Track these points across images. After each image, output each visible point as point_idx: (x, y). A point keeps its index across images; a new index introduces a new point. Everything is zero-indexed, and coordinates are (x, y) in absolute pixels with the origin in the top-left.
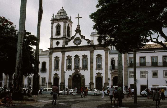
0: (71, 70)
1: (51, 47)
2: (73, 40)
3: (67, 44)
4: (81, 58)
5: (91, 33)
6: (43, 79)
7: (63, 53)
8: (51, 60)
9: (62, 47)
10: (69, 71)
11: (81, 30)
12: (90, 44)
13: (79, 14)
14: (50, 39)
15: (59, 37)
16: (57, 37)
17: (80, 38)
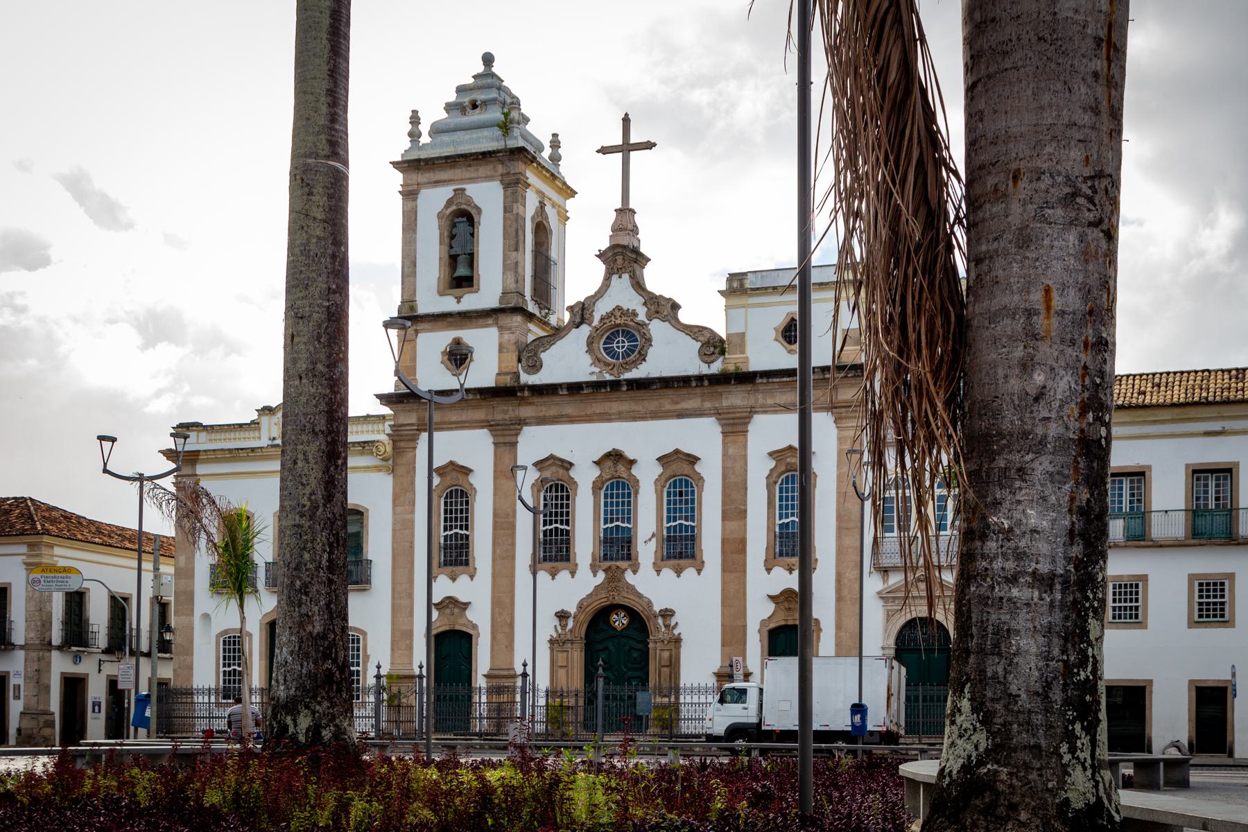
0: (573, 574)
2: (585, 330)
3: (535, 367)
4: (647, 475)
5: (732, 277)
7: (506, 438)
8: (403, 496)
9: (492, 384)
10: (553, 576)
11: (643, 250)
12: (716, 367)
13: (626, 121)
15: (471, 302)
16: (449, 304)
17: (642, 317)
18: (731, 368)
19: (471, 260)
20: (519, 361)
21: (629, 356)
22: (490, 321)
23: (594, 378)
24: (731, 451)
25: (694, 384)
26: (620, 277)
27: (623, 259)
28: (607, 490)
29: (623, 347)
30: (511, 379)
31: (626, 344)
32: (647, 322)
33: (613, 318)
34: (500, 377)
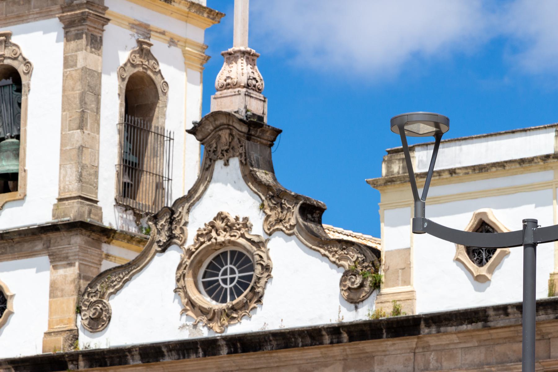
18: (387, 312)
20: (79, 310)
21: (239, 293)
22: (39, 246)
23: (185, 335)
25: (327, 339)
26: (226, 164)
27: (231, 134)
29: (232, 280)
30: (66, 340)
31: (237, 275)
33: (214, 234)
34: (49, 338)
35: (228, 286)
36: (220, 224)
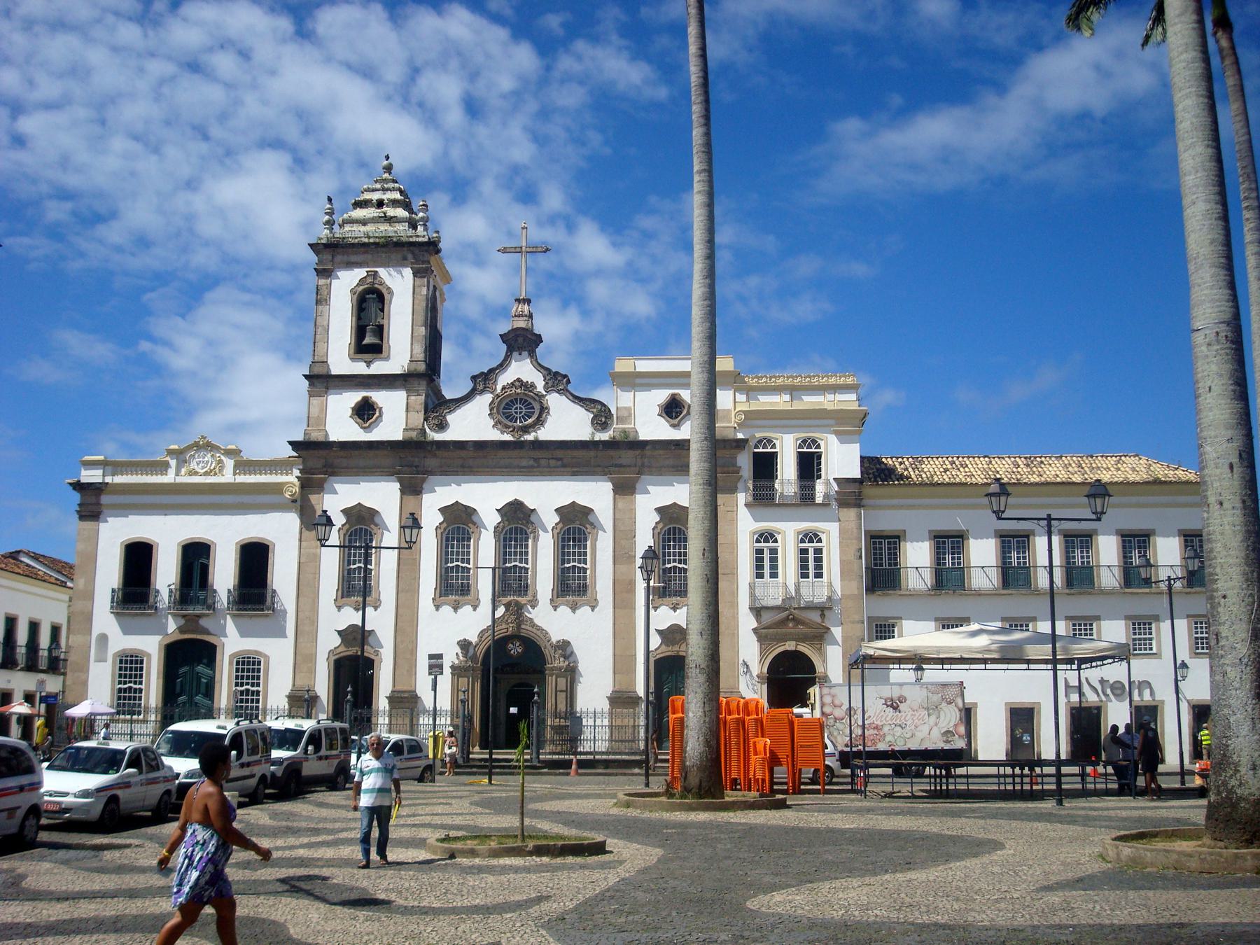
1: (316, 436)
2: (487, 398)
3: (442, 426)
6: (249, 668)
7: (412, 489)
9: (400, 438)
10: (456, 609)
14: (306, 376)
15: (379, 367)
16: (360, 368)
17: (540, 387)
19: (380, 331)
20: (426, 419)
24: (620, 505)
28: (506, 534)
32: (545, 393)
35: (518, 416)
36: (517, 383)
